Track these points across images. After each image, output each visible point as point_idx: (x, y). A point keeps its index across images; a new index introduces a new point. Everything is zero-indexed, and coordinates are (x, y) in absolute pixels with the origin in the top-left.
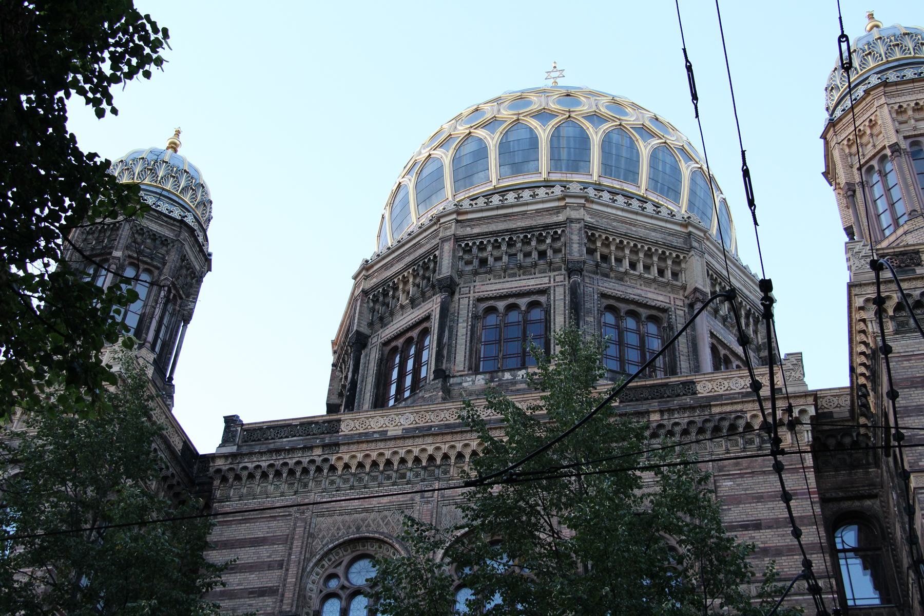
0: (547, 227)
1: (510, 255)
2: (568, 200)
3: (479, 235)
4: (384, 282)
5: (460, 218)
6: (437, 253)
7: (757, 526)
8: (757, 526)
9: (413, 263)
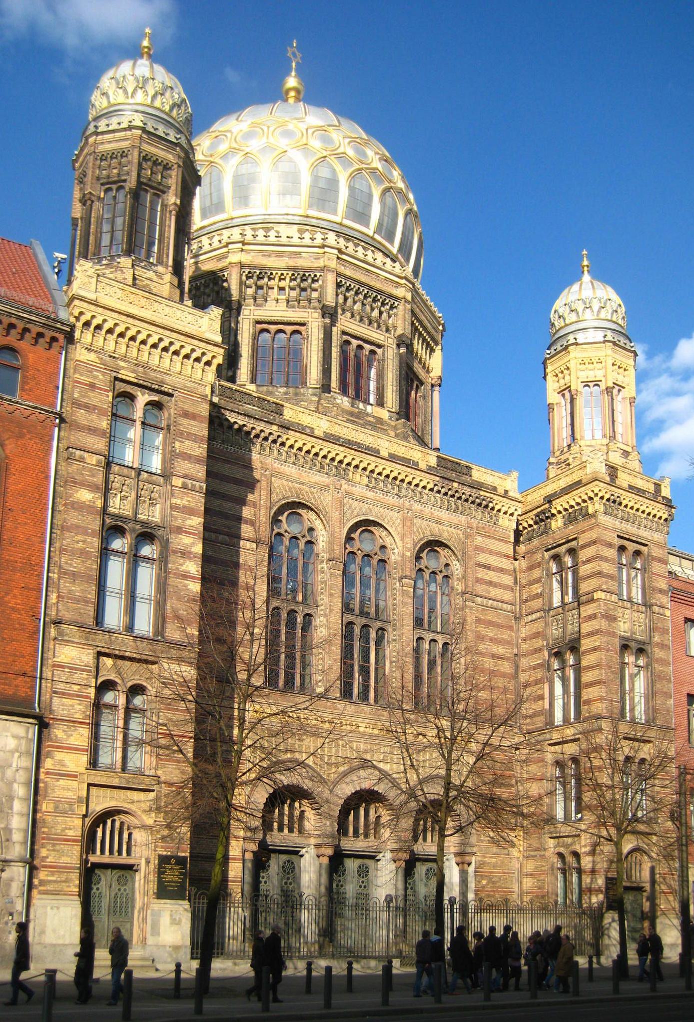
0: (391, 296)
1: (363, 304)
2: (403, 281)
3: (350, 278)
4: (262, 268)
6: (318, 274)
7: (488, 567)
8: (488, 567)
9: (294, 269)
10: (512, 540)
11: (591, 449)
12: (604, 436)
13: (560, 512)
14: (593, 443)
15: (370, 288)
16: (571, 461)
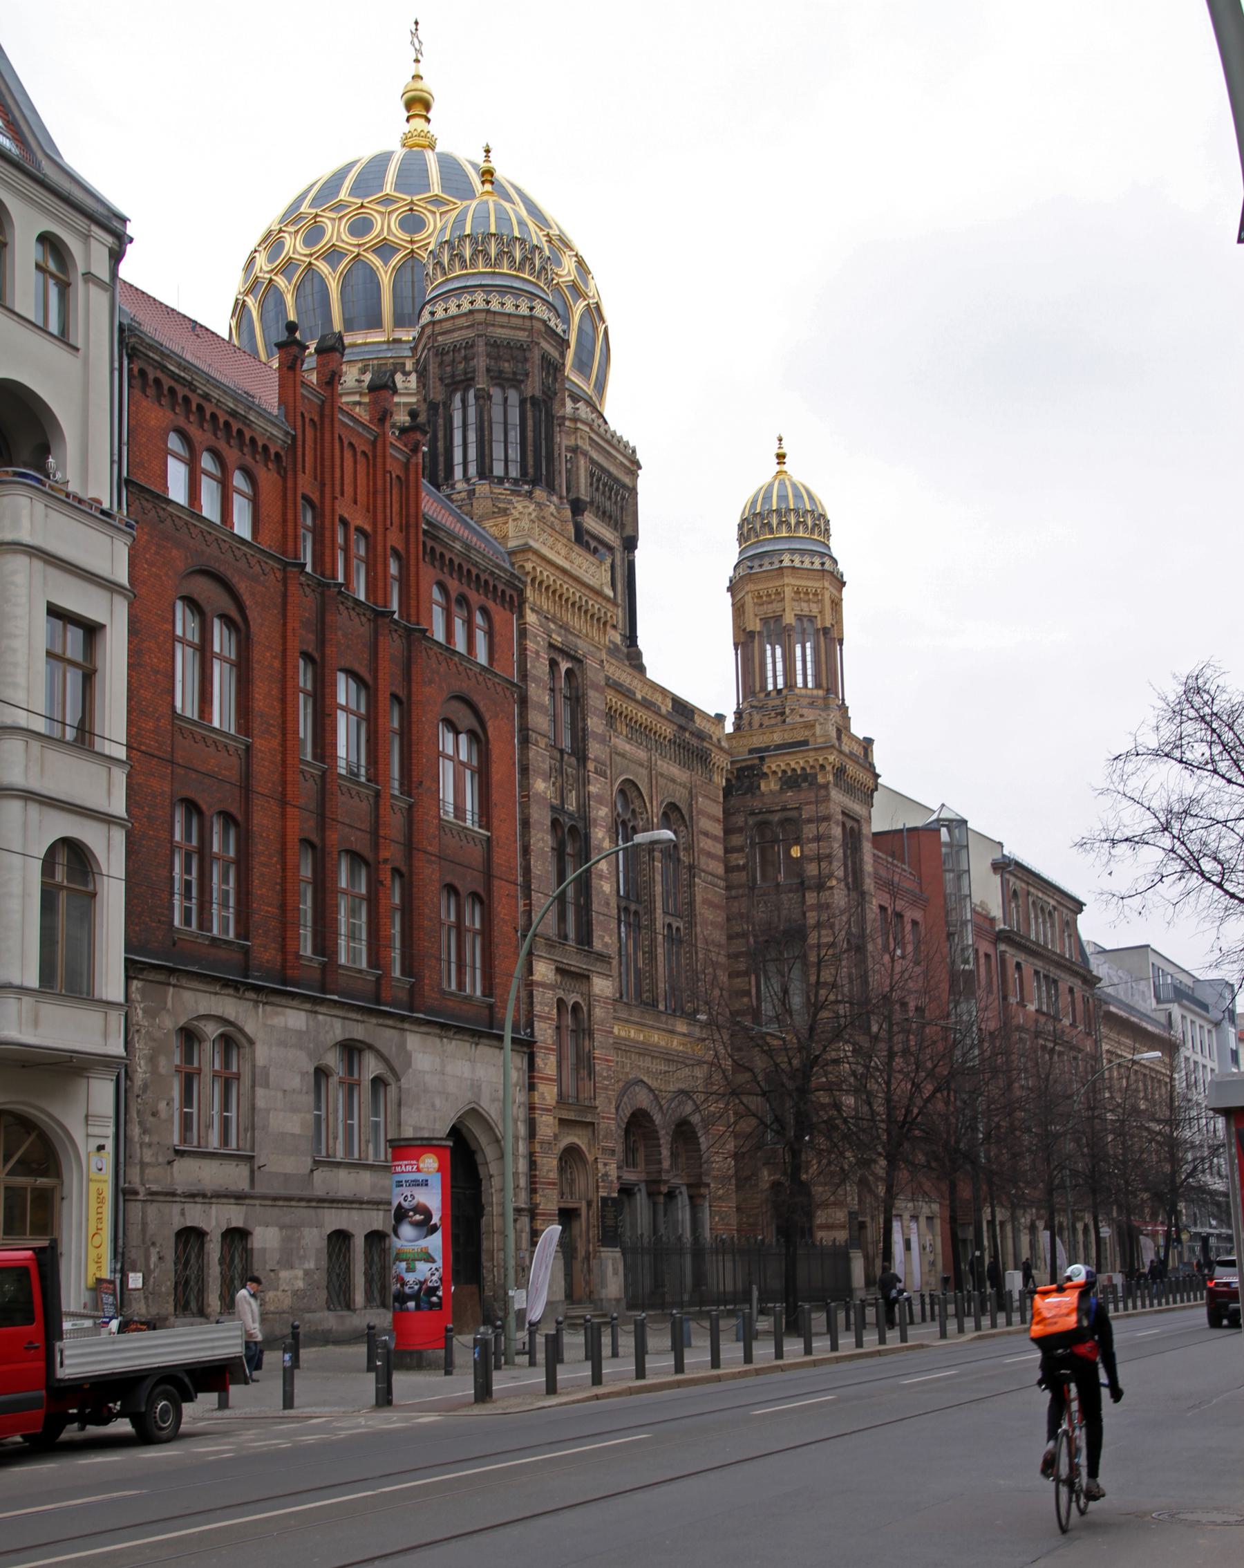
5: (593, 435)
10: (721, 799)
11: (807, 700)
12: (818, 685)
13: (775, 772)
14: (809, 692)
15: (610, 475)
16: (787, 711)
